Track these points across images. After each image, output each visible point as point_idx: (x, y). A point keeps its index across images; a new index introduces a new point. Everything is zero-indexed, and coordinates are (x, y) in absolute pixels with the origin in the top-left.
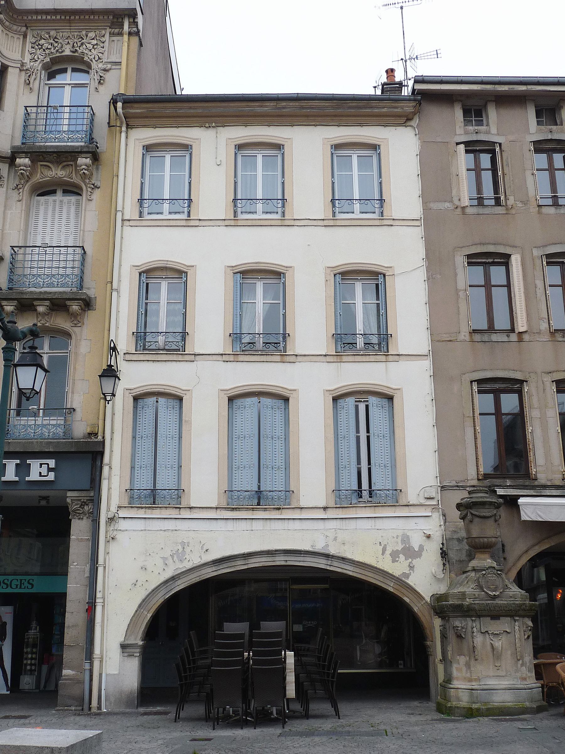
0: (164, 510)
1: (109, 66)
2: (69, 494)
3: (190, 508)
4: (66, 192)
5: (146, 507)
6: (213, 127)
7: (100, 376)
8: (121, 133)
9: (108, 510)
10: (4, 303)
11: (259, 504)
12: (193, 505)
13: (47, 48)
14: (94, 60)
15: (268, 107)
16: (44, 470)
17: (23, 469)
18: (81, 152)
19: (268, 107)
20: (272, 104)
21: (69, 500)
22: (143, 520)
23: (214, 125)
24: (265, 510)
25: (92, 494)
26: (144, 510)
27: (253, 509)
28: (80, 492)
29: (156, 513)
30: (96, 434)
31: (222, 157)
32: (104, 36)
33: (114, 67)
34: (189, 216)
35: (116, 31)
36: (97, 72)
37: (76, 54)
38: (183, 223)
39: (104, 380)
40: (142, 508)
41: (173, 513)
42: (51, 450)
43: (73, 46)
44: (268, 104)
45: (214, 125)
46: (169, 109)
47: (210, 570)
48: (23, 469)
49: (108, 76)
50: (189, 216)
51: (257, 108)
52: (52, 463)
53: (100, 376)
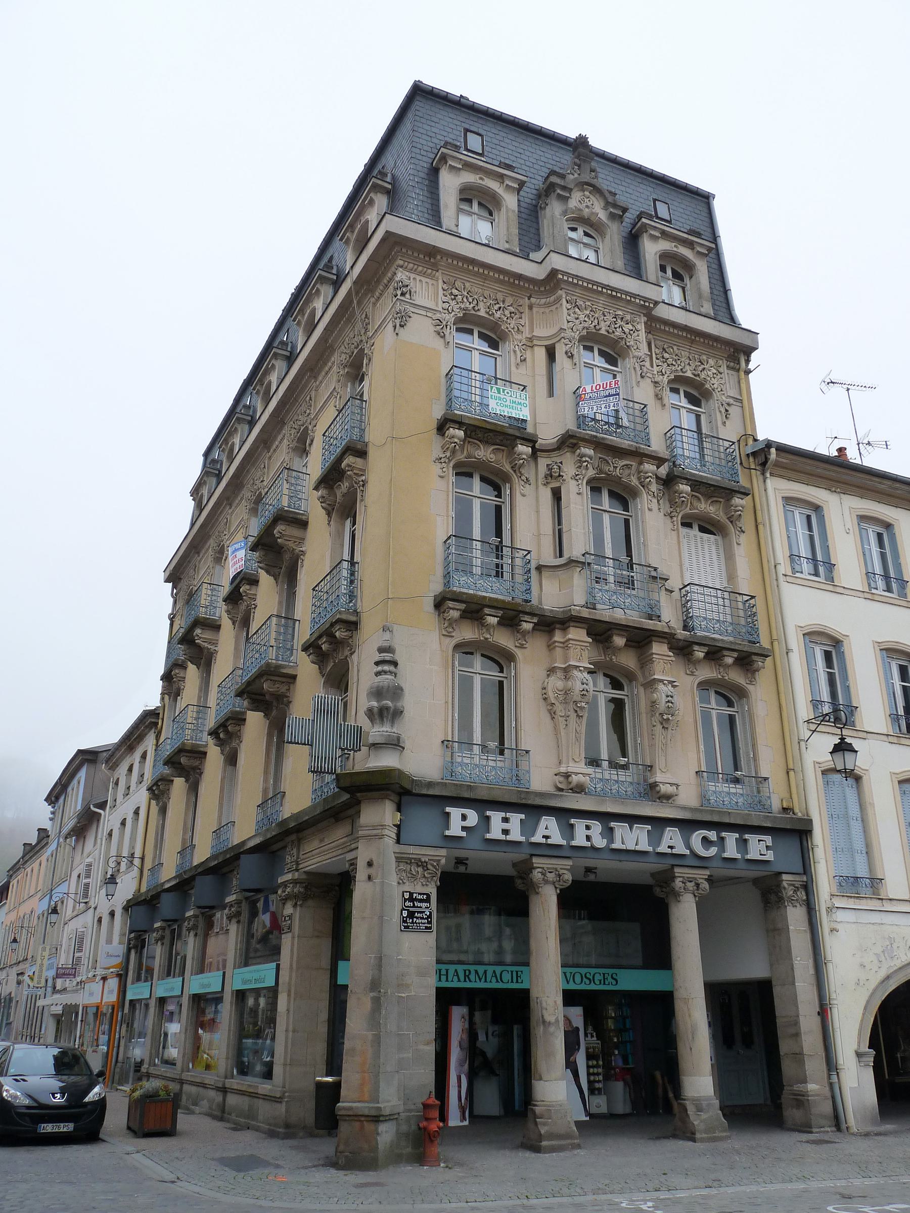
0: (869, 901)
1: (731, 401)
2: (784, 877)
3: (890, 900)
4: (703, 530)
5: (854, 897)
6: (839, 493)
7: (831, 753)
8: (765, 481)
12: (891, 897)
13: (672, 364)
14: (716, 390)
15: (885, 485)
17: (743, 844)
19: (885, 485)
20: (889, 483)
22: (853, 911)
23: (839, 490)
25: (805, 879)
26: (852, 899)
28: (794, 876)
31: (849, 525)
33: (735, 403)
36: (722, 405)
37: (698, 378)
39: (835, 755)
40: (851, 897)
41: (874, 904)
42: (769, 825)
44: (886, 482)
45: (839, 490)
46: (832, 473)
48: (743, 844)
51: (875, 483)
52: (768, 839)
53: (831, 753)
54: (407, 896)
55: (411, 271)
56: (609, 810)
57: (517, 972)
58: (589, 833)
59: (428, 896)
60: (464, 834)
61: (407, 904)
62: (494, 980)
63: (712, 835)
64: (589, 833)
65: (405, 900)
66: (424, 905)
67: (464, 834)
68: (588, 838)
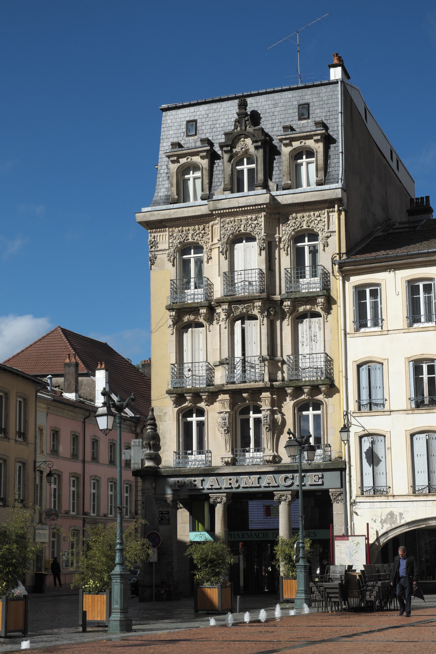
0: (379, 497)
1: (329, 234)
9: (351, 497)
10: (286, 389)
11: (429, 492)
16: (316, 478)
18: (319, 296)
21: (330, 494)
24: (433, 495)
27: (426, 495)
29: (376, 499)
30: (342, 458)
32: (324, 214)
33: (332, 234)
34: (382, 329)
35: (331, 209)
38: (379, 333)
43: (307, 223)
47: (405, 528)
49: (329, 240)
50: (382, 329)
54: (160, 513)
55: (155, 232)
56: (238, 471)
57: (266, 533)
58: (231, 482)
59: (168, 512)
60: (179, 488)
61: (161, 515)
62: (255, 537)
63: (290, 475)
64: (231, 482)
65: (160, 514)
66: (167, 515)
67: (179, 488)
68: (230, 484)
